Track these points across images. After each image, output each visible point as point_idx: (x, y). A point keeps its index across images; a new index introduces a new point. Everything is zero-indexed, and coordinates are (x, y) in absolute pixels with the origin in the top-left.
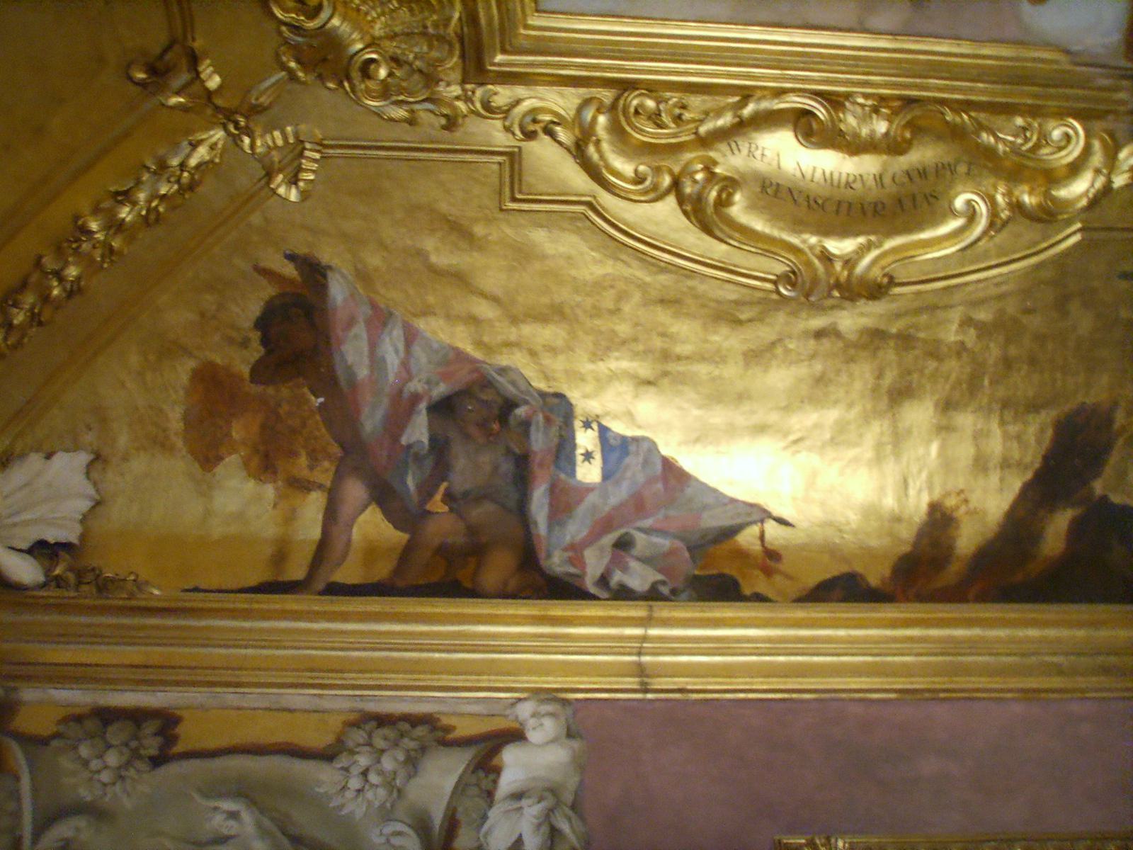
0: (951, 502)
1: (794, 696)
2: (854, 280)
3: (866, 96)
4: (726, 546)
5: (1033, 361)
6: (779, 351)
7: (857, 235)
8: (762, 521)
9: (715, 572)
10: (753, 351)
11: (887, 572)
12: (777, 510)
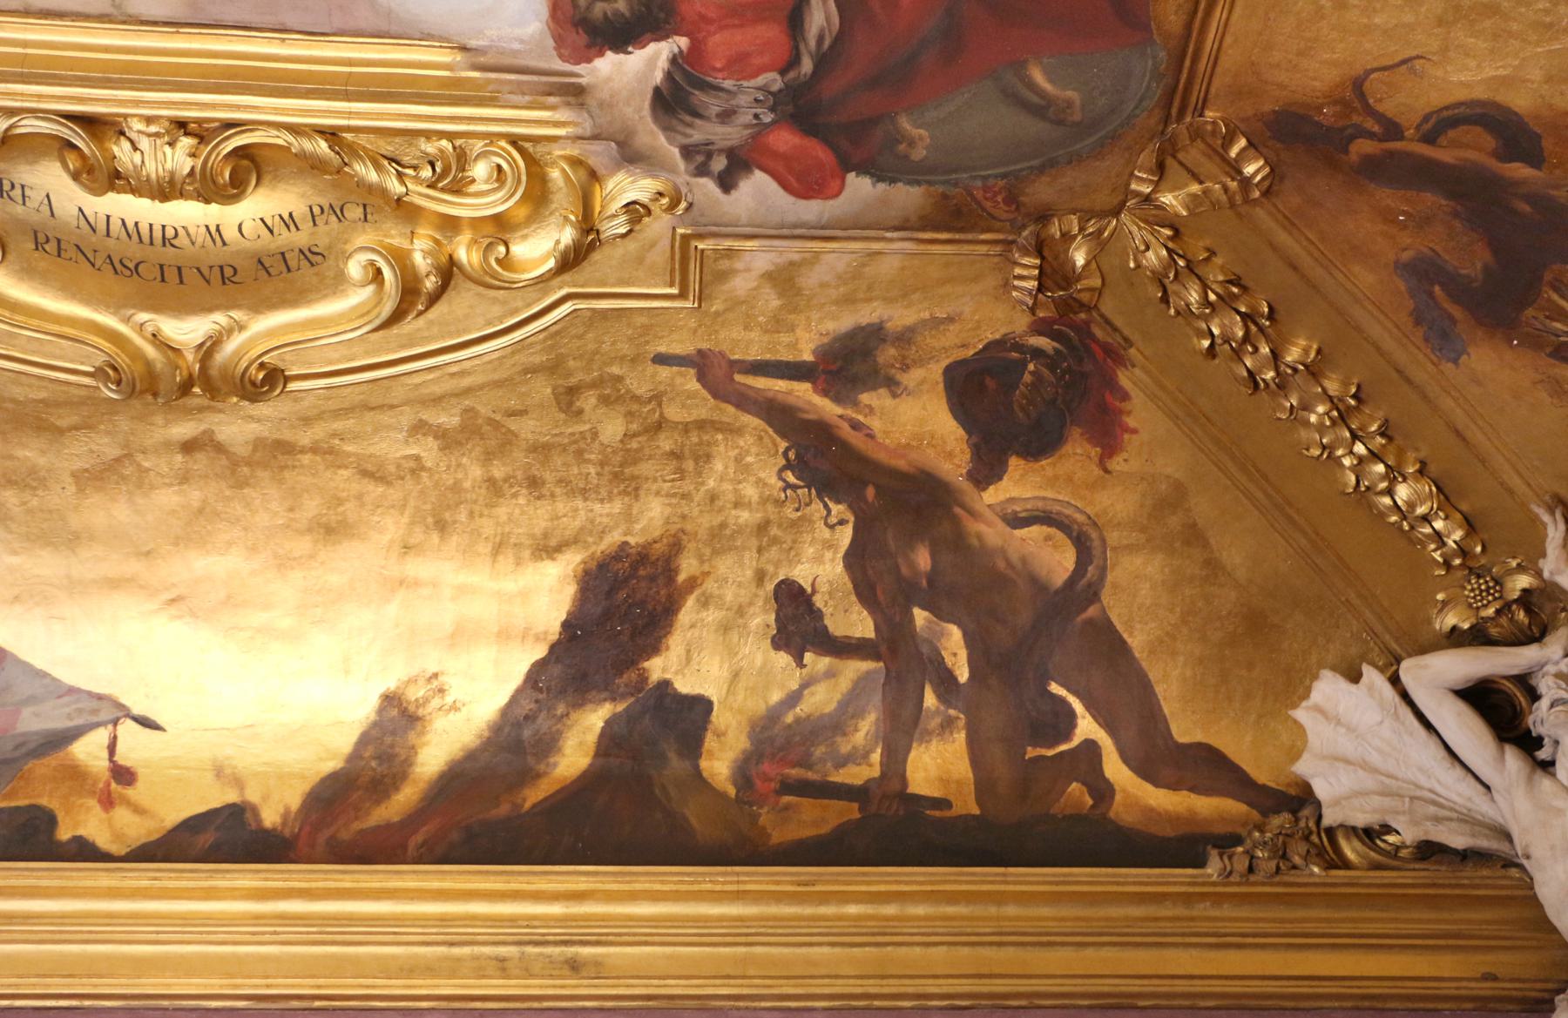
0: (415, 693)
1: (87, 1003)
2: (214, 372)
3: (149, 120)
4: (52, 761)
5: (534, 483)
6: (128, 471)
7: (210, 309)
8: (115, 723)
9: (22, 802)
10: (86, 470)
11: (295, 802)
12: (136, 711)
